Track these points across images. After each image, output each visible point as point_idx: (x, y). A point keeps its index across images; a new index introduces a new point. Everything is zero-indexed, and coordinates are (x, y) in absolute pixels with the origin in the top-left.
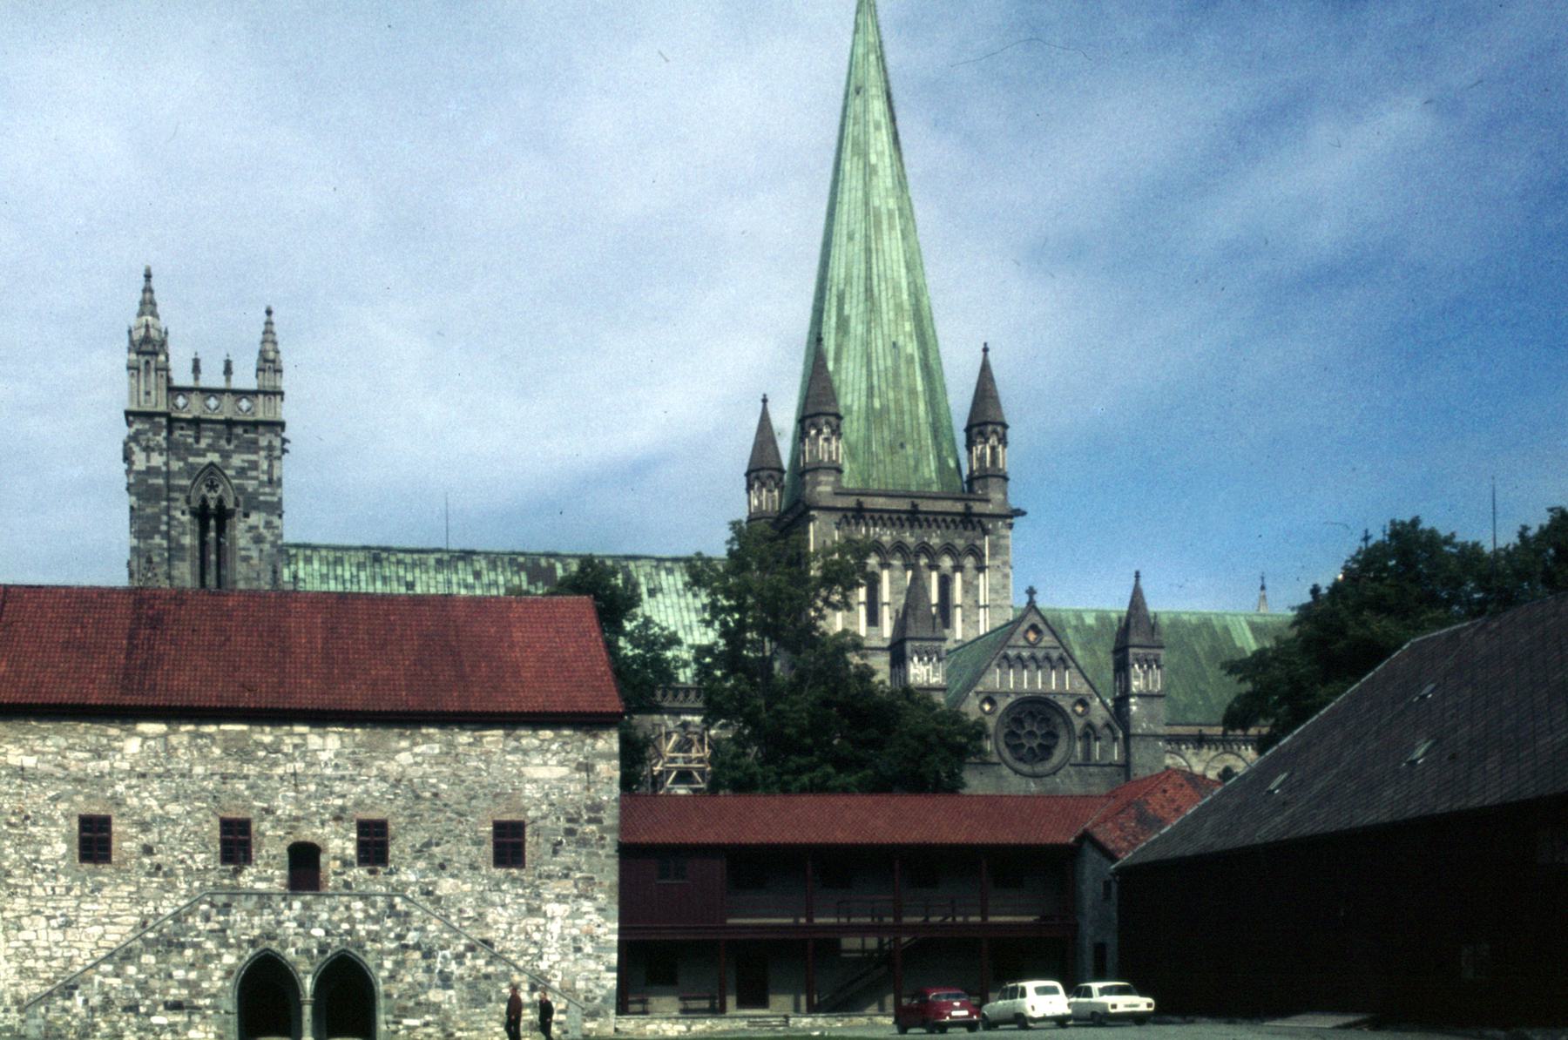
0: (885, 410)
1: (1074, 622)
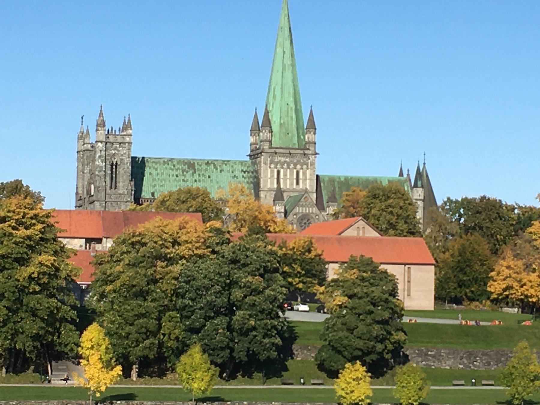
0: (284, 123)
1: (337, 180)
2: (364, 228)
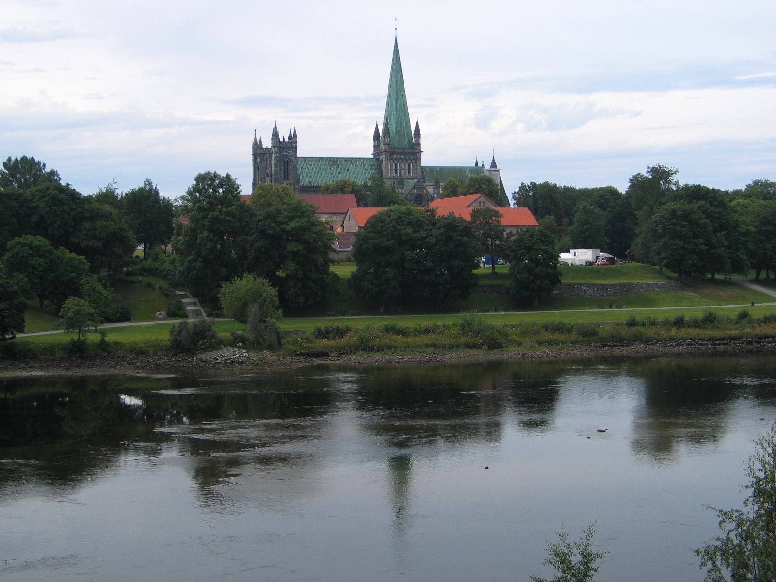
2: (484, 202)
